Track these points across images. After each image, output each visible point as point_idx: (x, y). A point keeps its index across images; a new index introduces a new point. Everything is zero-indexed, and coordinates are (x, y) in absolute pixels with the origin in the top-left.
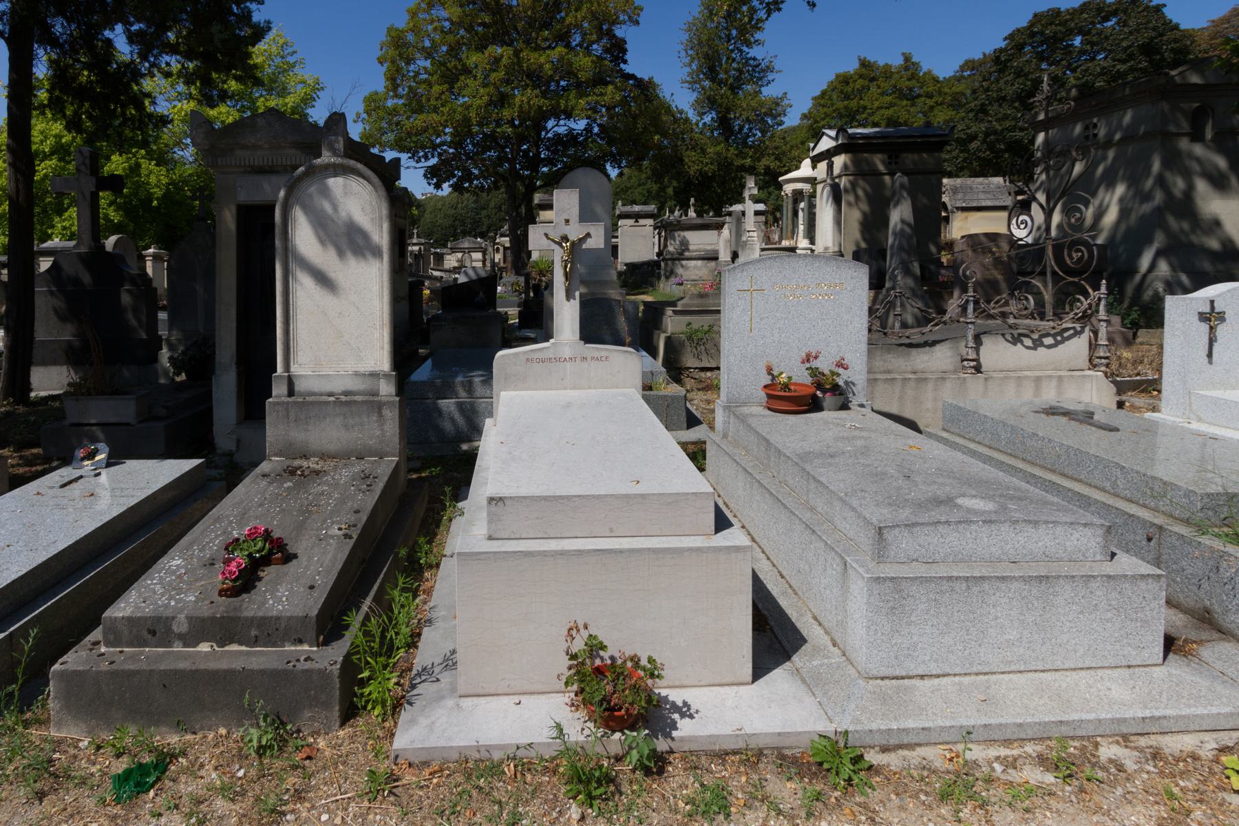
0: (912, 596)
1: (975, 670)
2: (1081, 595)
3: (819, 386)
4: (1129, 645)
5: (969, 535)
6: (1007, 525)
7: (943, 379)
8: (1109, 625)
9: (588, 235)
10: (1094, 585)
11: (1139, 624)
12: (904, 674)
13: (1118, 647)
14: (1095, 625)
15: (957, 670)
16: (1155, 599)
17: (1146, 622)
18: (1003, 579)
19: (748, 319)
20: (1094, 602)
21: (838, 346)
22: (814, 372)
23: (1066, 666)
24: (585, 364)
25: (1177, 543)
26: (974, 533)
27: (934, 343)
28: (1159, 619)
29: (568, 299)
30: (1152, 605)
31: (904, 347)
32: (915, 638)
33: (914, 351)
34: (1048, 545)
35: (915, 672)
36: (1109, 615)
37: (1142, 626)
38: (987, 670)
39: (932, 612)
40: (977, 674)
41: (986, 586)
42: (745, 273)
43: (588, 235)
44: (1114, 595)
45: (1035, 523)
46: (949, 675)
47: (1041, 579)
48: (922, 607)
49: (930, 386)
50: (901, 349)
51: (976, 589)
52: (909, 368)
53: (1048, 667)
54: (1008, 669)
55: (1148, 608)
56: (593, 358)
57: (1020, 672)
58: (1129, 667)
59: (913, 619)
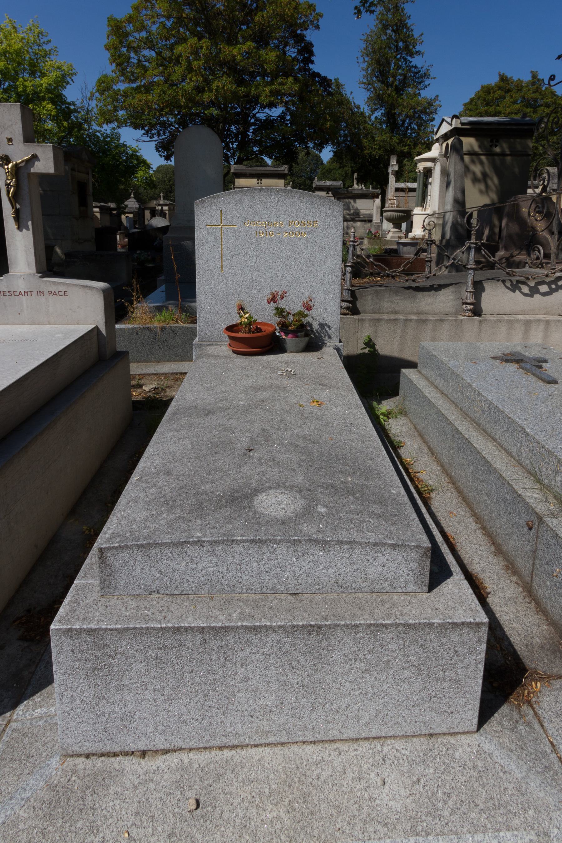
0: (122, 653)
1: (218, 743)
2: (367, 649)
3: (284, 326)
4: (432, 709)
5: (230, 559)
6: (284, 545)
7: (441, 320)
8: (406, 686)
9: (35, 157)
10: (384, 636)
11: (446, 685)
12: (117, 749)
13: (417, 710)
14: (385, 687)
15: (192, 744)
16: (471, 653)
17: (457, 682)
18: (255, 629)
19: (218, 256)
20: (385, 658)
21: (311, 286)
22: (280, 312)
23: (345, 736)
24: (42, 299)
25: (552, 542)
26: (237, 557)
27: (440, 287)
28: (475, 678)
29: (19, 228)
30: (466, 662)
31: (411, 291)
32: (130, 707)
33: (420, 294)
34: (342, 571)
35: (133, 747)
36: (406, 674)
37: (450, 687)
38: (236, 742)
39: (153, 673)
40: (221, 748)
41: (230, 639)
42: (214, 207)
43: (35, 157)
44: (414, 649)
45: (324, 544)
46: (181, 749)
47: (309, 629)
48: (137, 666)
49: (430, 327)
50: (408, 291)
51: (215, 644)
52: (415, 310)
53: (319, 737)
54: (264, 741)
55: (460, 665)
56: (50, 293)
57: (282, 744)
58: (431, 735)
59: (126, 681)
